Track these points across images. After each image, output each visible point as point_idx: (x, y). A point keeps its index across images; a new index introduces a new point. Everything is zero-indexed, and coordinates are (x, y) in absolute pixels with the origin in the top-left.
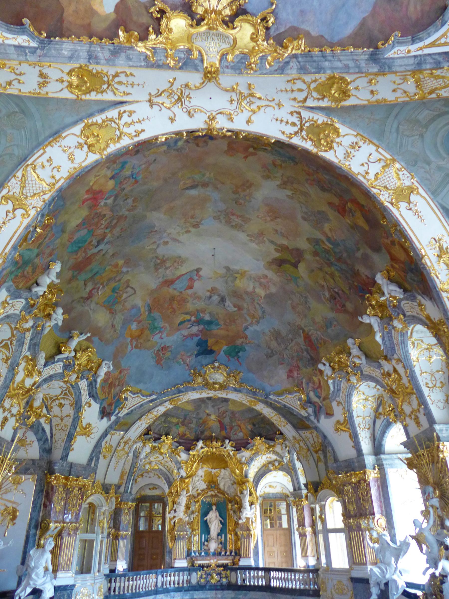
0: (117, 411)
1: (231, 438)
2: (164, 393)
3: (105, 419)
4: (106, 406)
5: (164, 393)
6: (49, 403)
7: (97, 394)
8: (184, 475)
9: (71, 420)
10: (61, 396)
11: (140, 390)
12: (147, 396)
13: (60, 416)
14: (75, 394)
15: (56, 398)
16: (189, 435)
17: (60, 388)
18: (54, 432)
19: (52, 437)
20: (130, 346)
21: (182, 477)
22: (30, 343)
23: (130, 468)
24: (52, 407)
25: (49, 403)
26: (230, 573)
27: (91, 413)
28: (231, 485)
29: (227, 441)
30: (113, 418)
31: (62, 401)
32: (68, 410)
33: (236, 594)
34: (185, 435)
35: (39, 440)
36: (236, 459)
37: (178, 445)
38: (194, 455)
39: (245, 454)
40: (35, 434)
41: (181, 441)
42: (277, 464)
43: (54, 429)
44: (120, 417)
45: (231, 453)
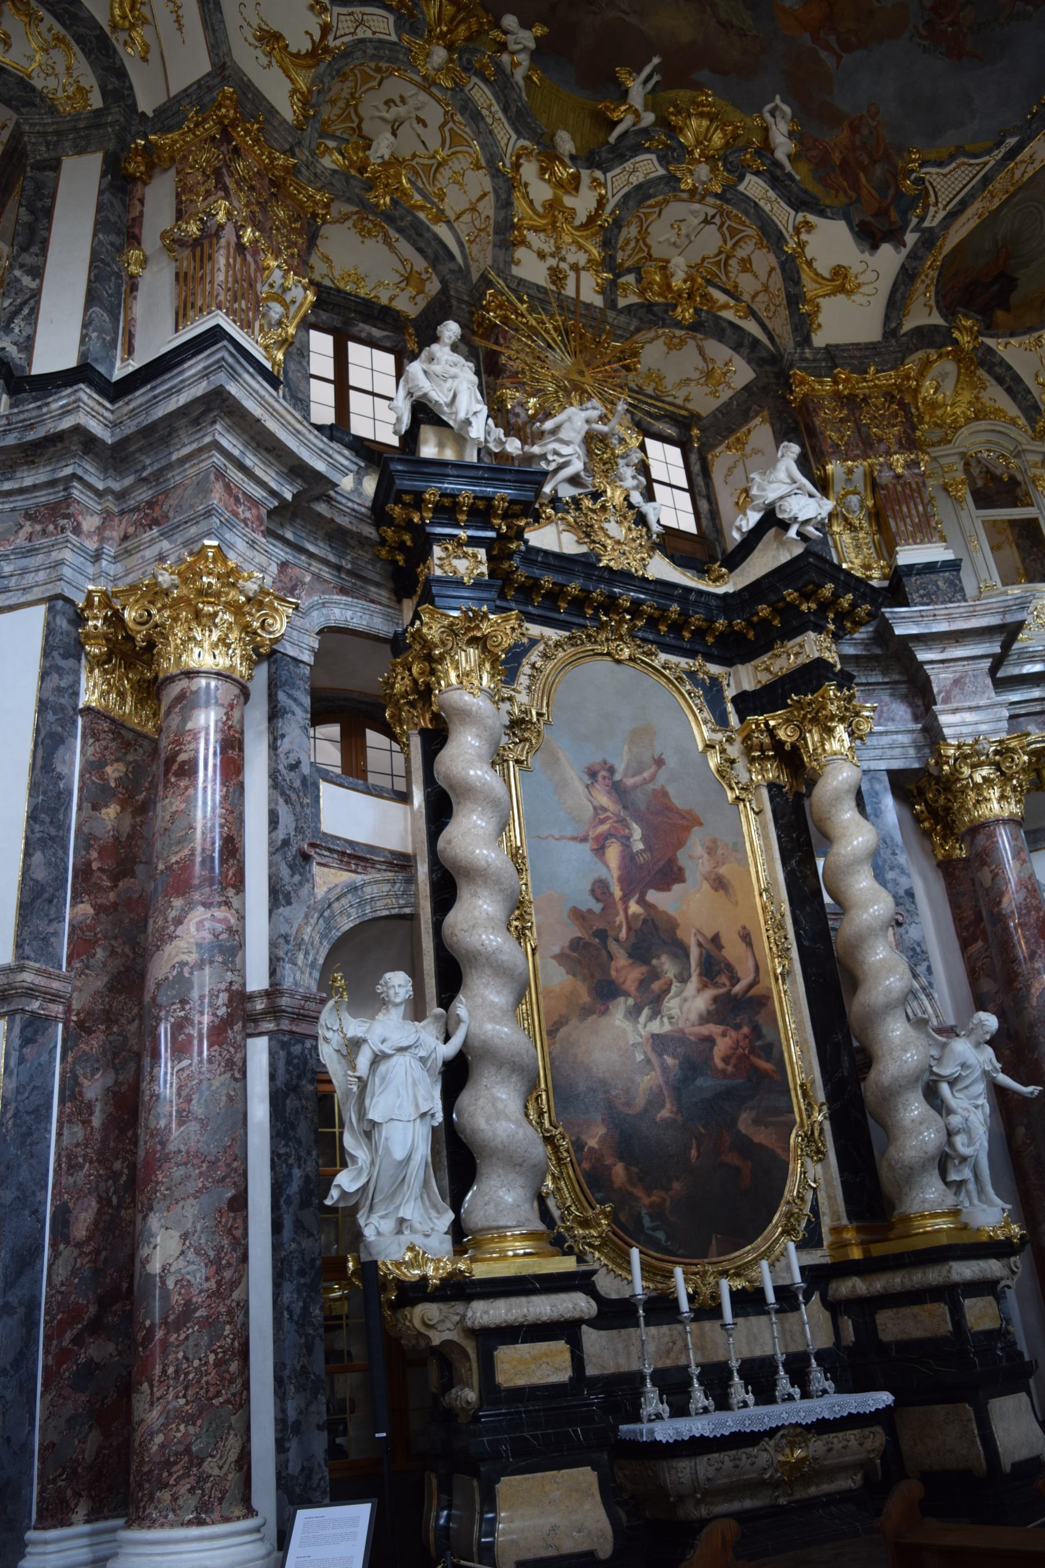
0: (915, 221)
2: (1034, 115)
3: (886, 248)
4: (868, 218)
5: (1034, 115)
6: (724, 278)
7: (806, 192)
9: (778, 271)
10: (730, 244)
11: (958, 148)
12: (989, 152)
13: (760, 288)
14: (746, 213)
15: (723, 256)
17: (706, 221)
18: (770, 326)
19: (771, 338)
20: (823, 54)
22: (508, 119)
24: (736, 286)
25: (724, 278)
27: (829, 242)
30: (911, 238)
31: (740, 253)
32: (764, 260)
35: (737, 348)
40: (720, 341)
43: (767, 322)
44: (931, 229)
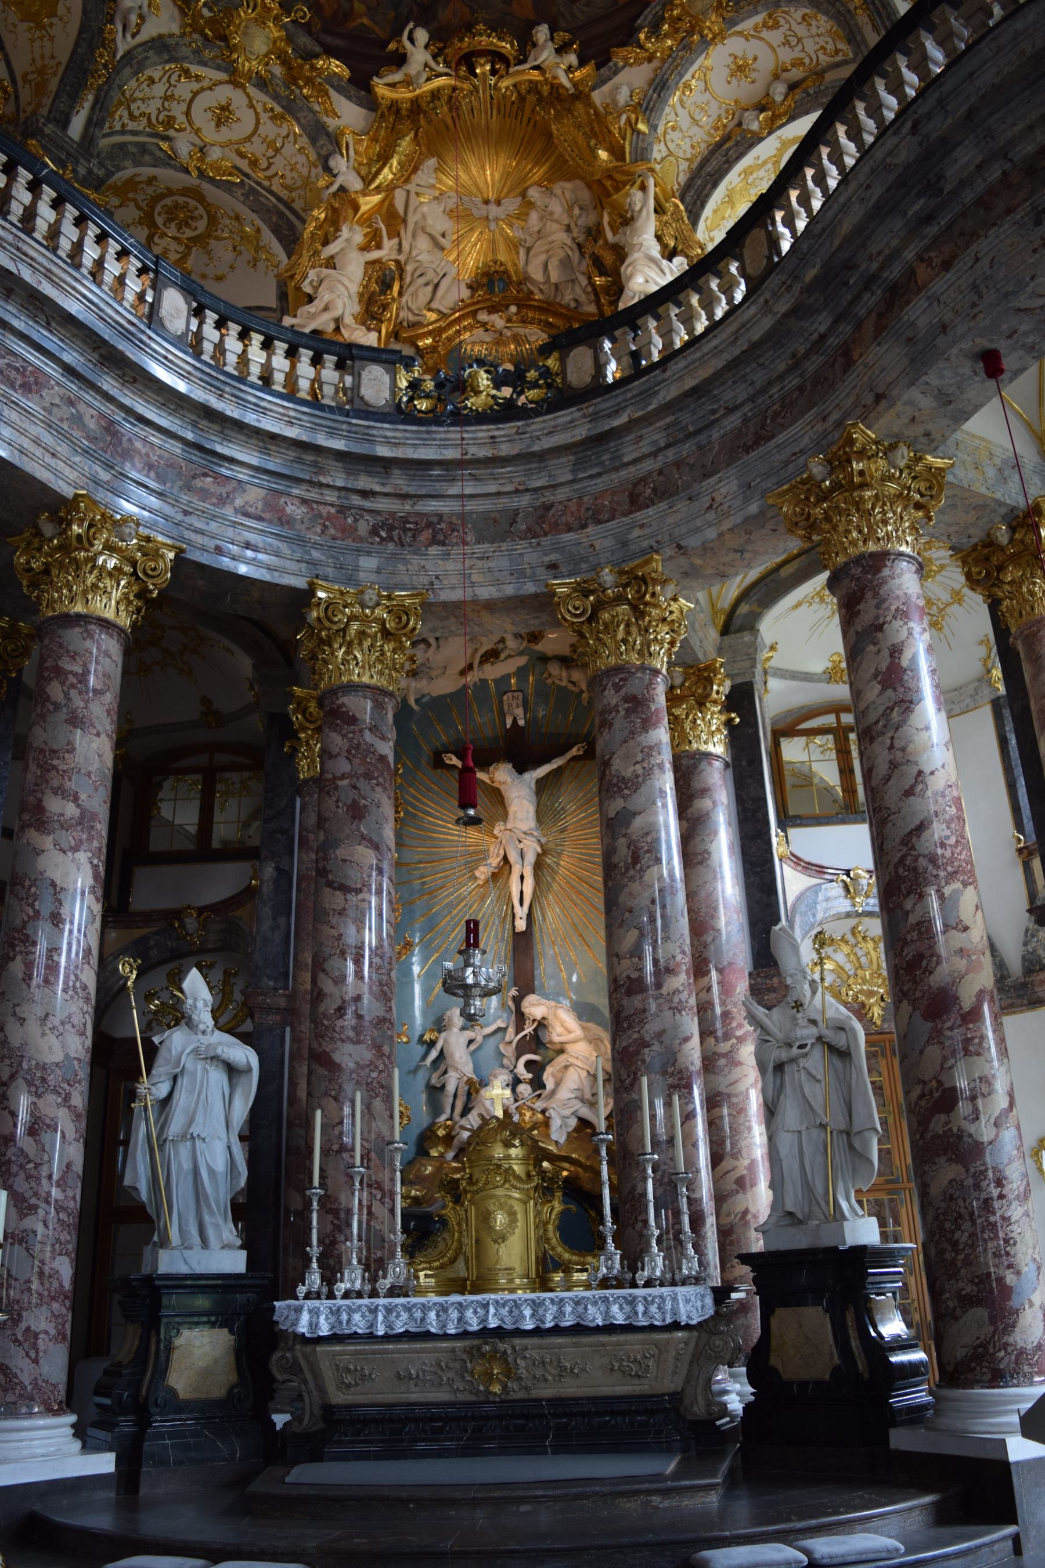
1: (563, 24)
8: (355, 184)
16: (365, 21)
21: (342, 189)
23: (77, 44)
26: (563, 362)
28: (575, 256)
29: (542, 33)
33: (594, 418)
34: (349, 15)
36: (589, 103)
37: (318, 49)
38: (394, 106)
39: (630, 80)
41: (328, 39)
42: (779, 91)
45: (564, 80)
